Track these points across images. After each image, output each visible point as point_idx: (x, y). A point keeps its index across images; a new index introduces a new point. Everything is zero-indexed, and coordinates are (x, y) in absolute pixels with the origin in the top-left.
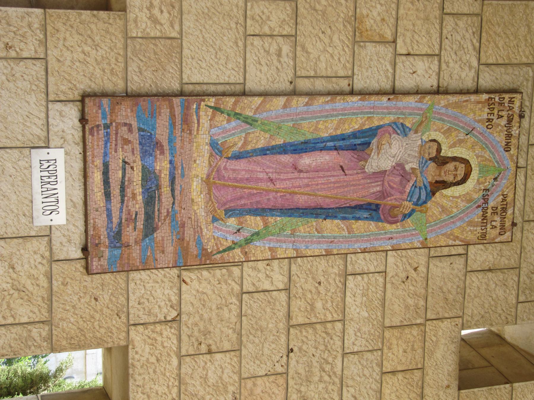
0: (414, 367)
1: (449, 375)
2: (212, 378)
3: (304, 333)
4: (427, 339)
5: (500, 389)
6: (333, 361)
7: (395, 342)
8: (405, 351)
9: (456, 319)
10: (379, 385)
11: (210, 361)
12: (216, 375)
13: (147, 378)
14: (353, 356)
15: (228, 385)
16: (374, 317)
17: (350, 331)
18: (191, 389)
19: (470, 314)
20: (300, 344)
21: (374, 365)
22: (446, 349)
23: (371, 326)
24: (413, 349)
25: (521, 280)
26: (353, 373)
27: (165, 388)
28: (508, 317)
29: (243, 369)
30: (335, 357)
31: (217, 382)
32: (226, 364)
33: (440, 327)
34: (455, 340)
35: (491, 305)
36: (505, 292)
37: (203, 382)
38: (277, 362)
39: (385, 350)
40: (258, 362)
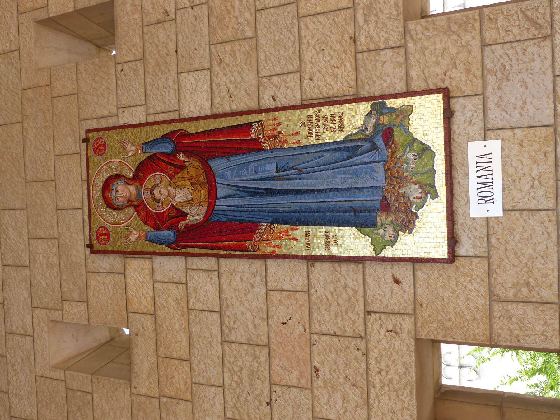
0: (165, 360)
1: (137, 345)
2: (338, 396)
3: (258, 416)
4: (157, 382)
5: (97, 322)
6: (232, 383)
7: (182, 387)
8: (173, 377)
9: (136, 393)
10: (192, 351)
11: (340, 414)
12: (335, 400)
13: (400, 415)
14: (216, 384)
15: (323, 386)
16: (201, 414)
17: (219, 407)
18: (358, 392)
19: (126, 395)
20: (260, 407)
21: (197, 370)
22: (141, 369)
23: (202, 407)
24: (167, 377)
25: (91, 412)
26: (215, 367)
27: (382, 401)
28: (97, 383)
29: (310, 398)
30: (230, 385)
31: (333, 393)
32: (325, 407)
33: (148, 389)
34: (135, 374)
35: (112, 397)
36: (102, 406)
37: (346, 396)
38: (280, 397)
39: (189, 381)
40: (298, 402)
